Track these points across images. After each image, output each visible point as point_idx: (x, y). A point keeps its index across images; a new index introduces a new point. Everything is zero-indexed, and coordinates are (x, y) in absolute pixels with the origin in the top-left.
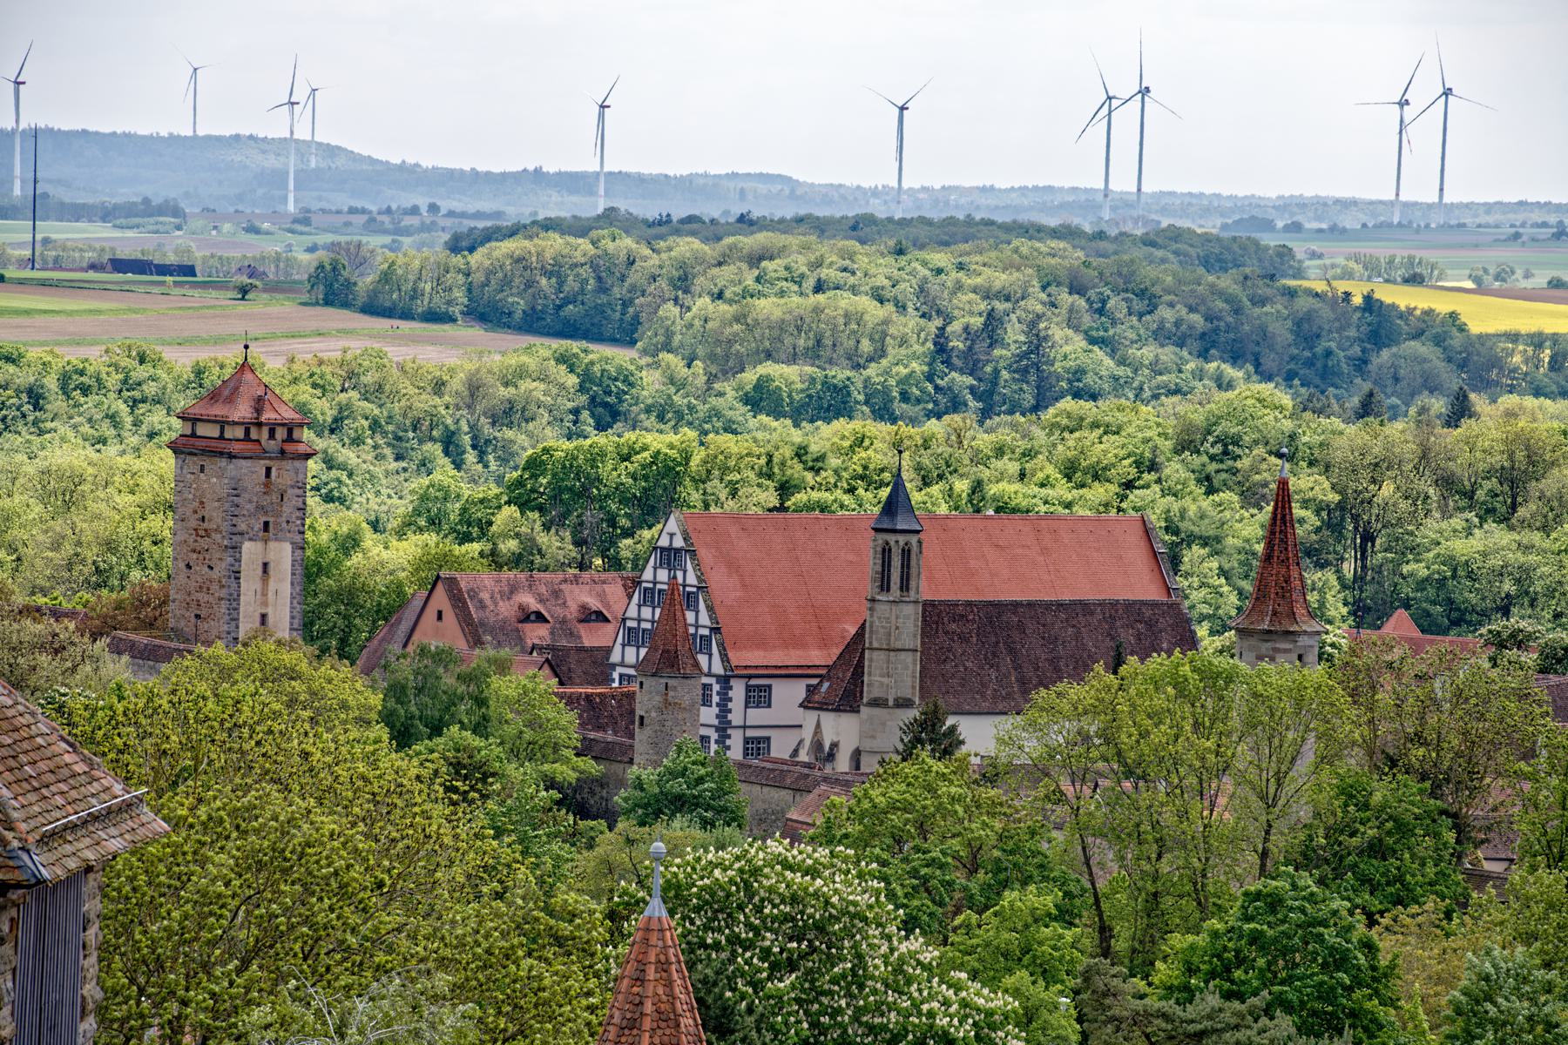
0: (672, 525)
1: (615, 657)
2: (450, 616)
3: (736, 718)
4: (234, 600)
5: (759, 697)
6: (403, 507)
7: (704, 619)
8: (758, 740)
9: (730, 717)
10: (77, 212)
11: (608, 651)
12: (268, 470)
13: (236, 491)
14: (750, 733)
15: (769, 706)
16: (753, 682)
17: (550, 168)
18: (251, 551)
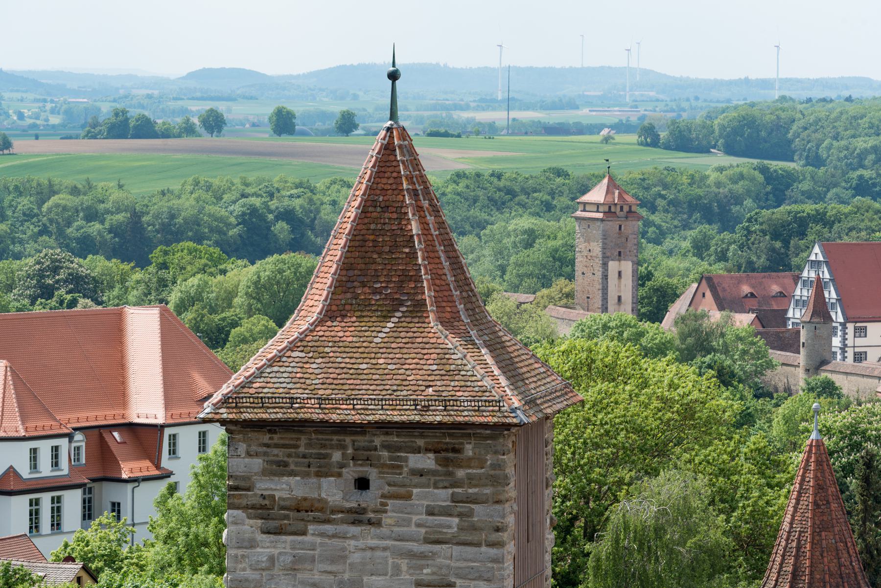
0: (817, 249)
1: (790, 314)
2: (708, 294)
3: (849, 342)
4: (605, 290)
5: (861, 332)
6: (686, 244)
7: (834, 295)
8: (861, 353)
9: (847, 342)
10: (527, 107)
11: (786, 311)
12: (620, 226)
13: (605, 237)
14: (857, 350)
15: (866, 336)
16: (858, 325)
17: (753, 77)
18: (613, 266)
